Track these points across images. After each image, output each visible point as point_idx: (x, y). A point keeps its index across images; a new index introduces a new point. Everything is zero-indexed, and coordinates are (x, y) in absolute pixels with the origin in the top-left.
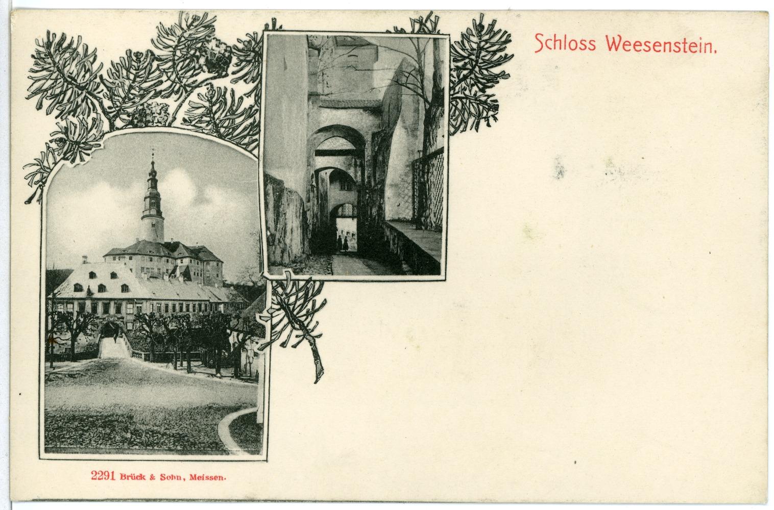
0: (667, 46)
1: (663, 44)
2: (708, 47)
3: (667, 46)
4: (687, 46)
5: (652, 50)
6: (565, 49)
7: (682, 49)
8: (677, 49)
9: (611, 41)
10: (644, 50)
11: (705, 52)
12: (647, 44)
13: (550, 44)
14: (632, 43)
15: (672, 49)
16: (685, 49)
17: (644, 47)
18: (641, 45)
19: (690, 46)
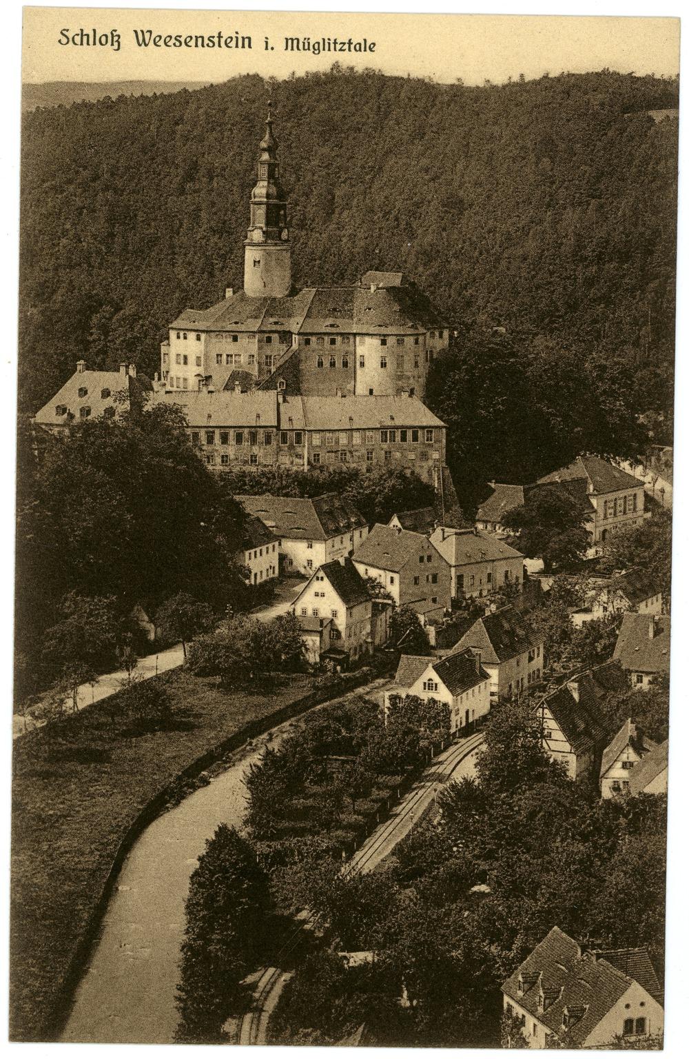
1: (194, 38)
2: (247, 41)
4: (223, 41)
5: (183, 44)
6: (95, 44)
7: (217, 44)
8: (211, 44)
10: (174, 44)
11: (243, 47)
13: (78, 39)
15: (205, 45)
17: (173, 41)
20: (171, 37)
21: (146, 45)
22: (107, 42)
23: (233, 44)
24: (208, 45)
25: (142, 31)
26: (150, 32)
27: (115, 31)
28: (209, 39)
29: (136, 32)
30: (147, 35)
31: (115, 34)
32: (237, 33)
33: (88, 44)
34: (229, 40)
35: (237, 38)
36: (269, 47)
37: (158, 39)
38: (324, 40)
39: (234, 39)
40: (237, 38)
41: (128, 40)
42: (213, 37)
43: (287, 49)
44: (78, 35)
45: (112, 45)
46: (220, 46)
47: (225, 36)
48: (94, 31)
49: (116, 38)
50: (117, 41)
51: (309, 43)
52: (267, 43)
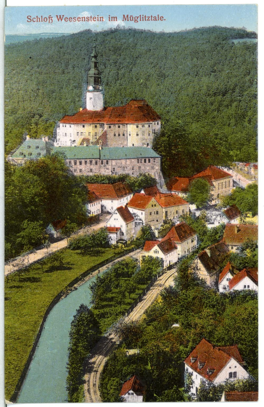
0: (83, 18)
3: (83, 18)
4: (92, 18)
9: (59, 17)
12: (75, 18)
15: (86, 20)
17: (73, 20)
18: (72, 19)
27: (50, 16)
35: (98, 18)
39: (97, 18)
40: (98, 18)
41: (55, 19)
48: (42, 17)
50: (51, 19)
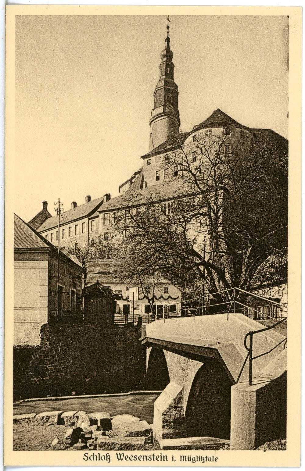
0: (145, 457)
1: (142, 457)
2: (165, 457)
3: (145, 457)
4: (155, 458)
6: (99, 460)
8: (150, 459)
10: (134, 459)
11: (164, 460)
13: (92, 458)
14: (129, 457)
16: (153, 458)
17: (133, 458)
19: (156, 457)
20: (132, 456)
21: (122, 460)
22: (104, 459)
23: (159, 459)
24: (148, 459)
25: (120, 454)
26: (123, 454)
27: (108, 454)
28: (149, 457)
29: (117, 454)
30: (122, 456)
31: (108, 455)
32: (161, 454)
33: (96, 460)
34: (158, 457)
35: (161, 456)
36: (174, 460)
37: (126, 457)
38: (197, 456)
39: (160, 457)
40: (161, 456)
42: (151, 456)
43: (181, 461)
44: (92, 456)
45: (107, 460)
46: (154, 460)
47: (156, 455)
49: (108, 457)
51: (191, 458)
52: (173, 458)
